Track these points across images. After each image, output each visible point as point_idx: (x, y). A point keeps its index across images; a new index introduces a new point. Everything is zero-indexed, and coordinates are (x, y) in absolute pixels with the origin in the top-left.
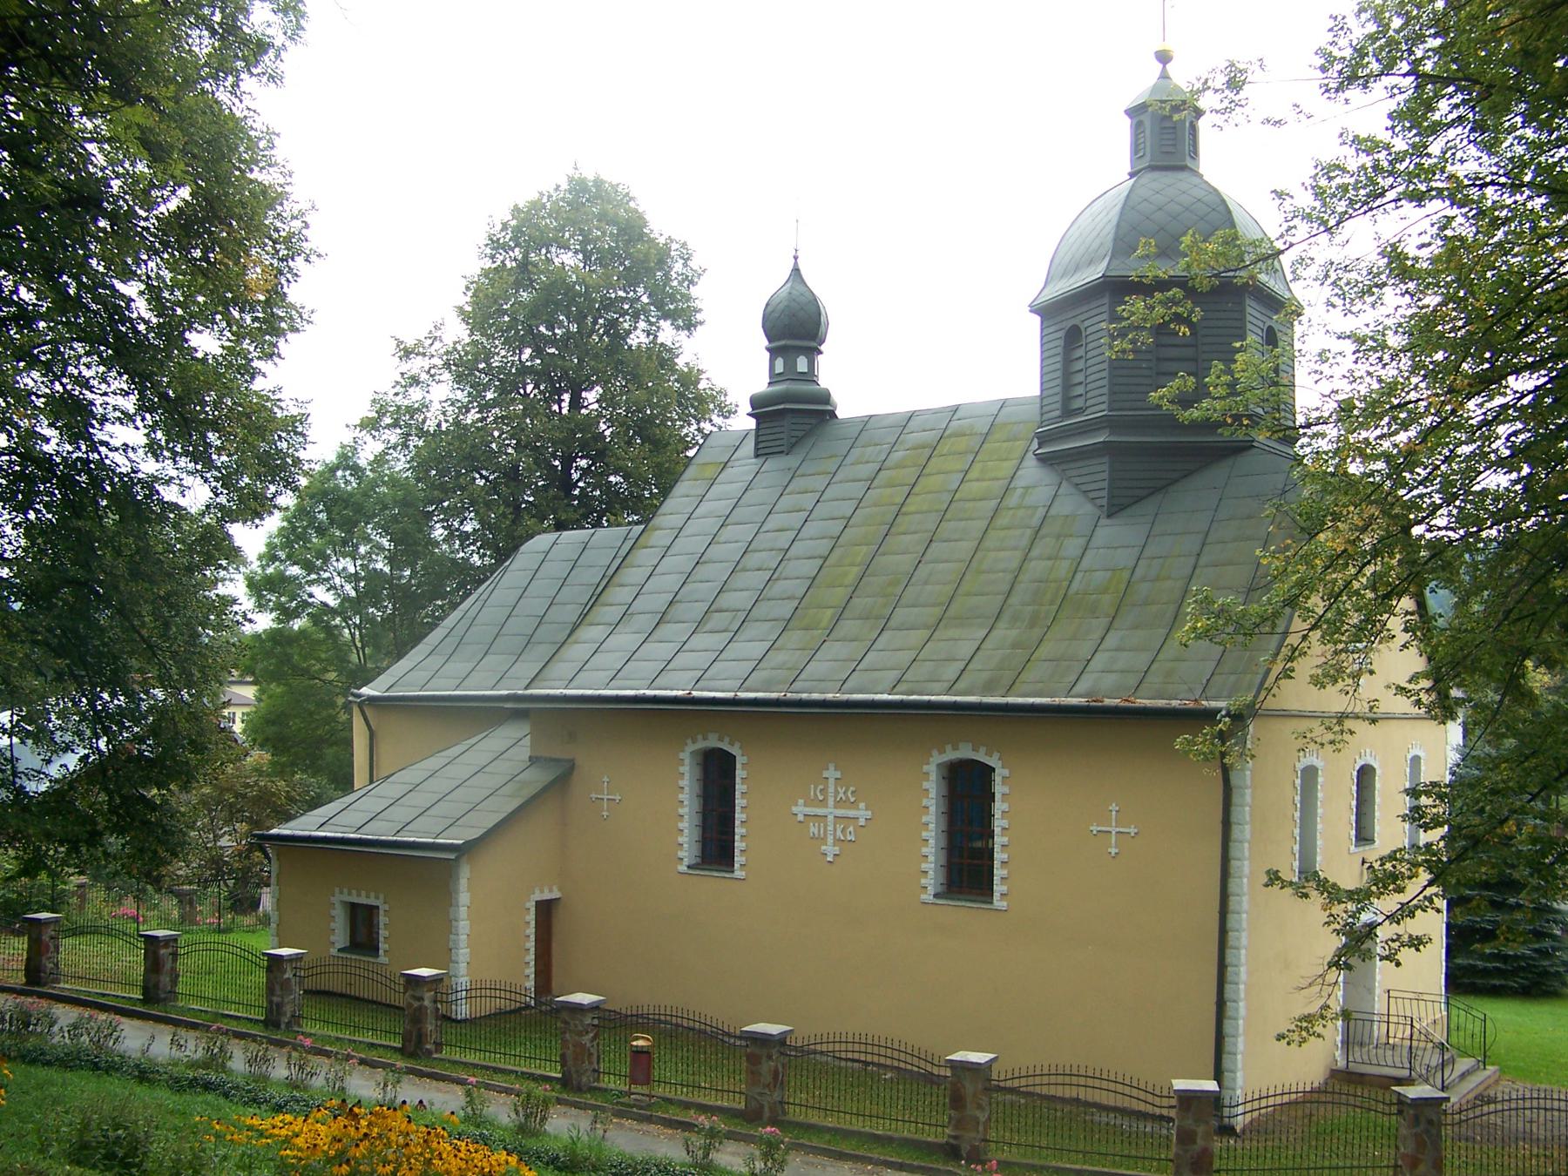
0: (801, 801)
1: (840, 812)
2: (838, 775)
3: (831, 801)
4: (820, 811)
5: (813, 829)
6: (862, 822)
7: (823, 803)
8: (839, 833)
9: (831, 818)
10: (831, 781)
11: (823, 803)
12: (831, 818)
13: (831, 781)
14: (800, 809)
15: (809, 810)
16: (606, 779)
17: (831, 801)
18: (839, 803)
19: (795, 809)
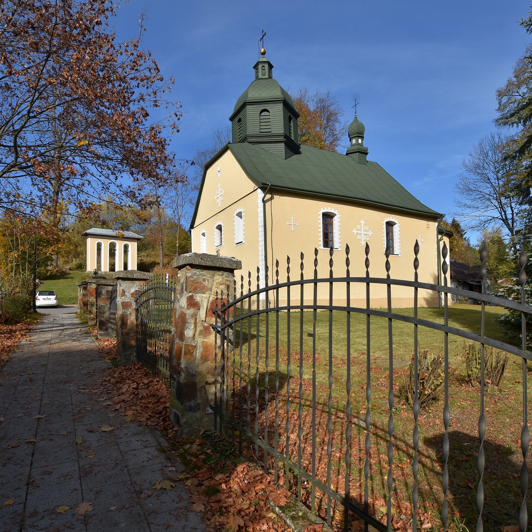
0: (355, 229)
1: (365, 233)
2: (364, 223)
3: (363, 231)
4: (359, 232)
5: (359, 237)
6: (370, 235)
7: (360, 230)
8: (365, 239)
9: (363, 234)
10: (362, 224)
11: (360, 230)
12: (363, 234)
13: (362, 224)
14: (355, 231)
15: (357, 232)
16: (292, 218)
17: (363, 231)
18: (365, 230)
19: (353, 231)
